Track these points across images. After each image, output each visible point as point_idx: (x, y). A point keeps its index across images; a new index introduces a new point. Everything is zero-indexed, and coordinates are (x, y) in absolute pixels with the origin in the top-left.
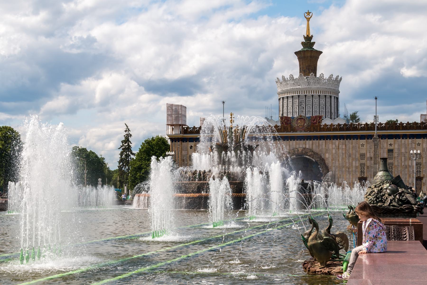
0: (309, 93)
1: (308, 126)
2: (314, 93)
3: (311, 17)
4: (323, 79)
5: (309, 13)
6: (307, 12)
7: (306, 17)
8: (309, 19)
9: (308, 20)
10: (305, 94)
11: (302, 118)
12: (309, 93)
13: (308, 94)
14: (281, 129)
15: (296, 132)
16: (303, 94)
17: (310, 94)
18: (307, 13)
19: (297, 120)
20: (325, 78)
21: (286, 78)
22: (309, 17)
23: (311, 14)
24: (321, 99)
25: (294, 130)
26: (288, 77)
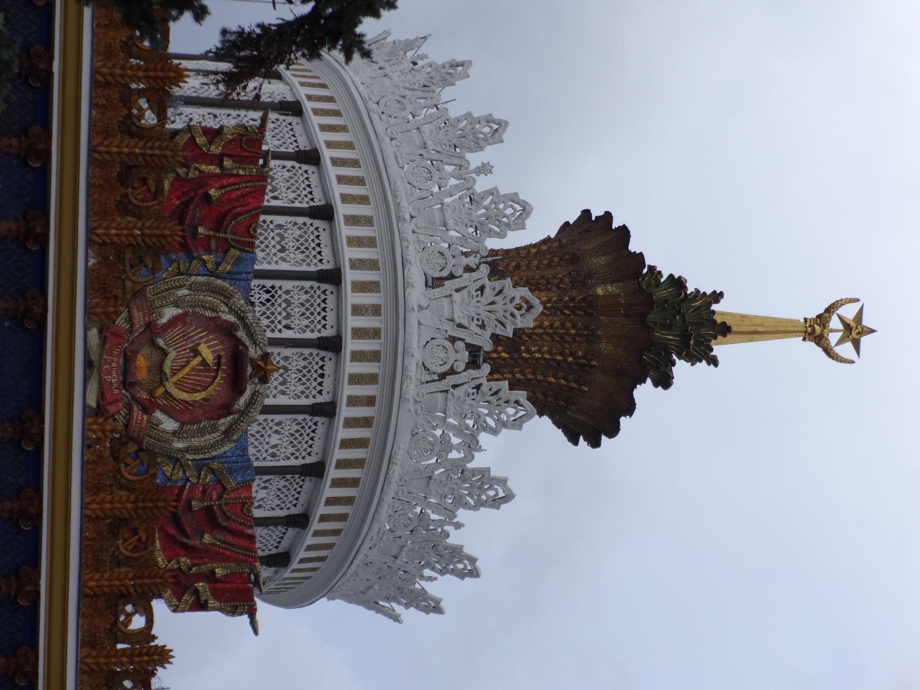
0: (356, 379)
1: (150, 454)
2: (350, 423)
3: (829, 352)
4: (459, 502)
5: (855, 332)
6: (865, 322)
7: (830, 310)
8: (820, 340)
9: (815, 331)
10: (351, 345)
11: (237, 387)
12: (356, 379)
13: (351, 367)
14: (131, 128)
15: (88, 313)
16: (352, 322)
17: (349, 390)
18: (859, 316)
19: (226, 331)
20: (462, 515)
21: (488, 154)
22: (833, 338)
23: (846, 350)
24: (277, 482)
25: (109, 292)
26: (502, 180)
